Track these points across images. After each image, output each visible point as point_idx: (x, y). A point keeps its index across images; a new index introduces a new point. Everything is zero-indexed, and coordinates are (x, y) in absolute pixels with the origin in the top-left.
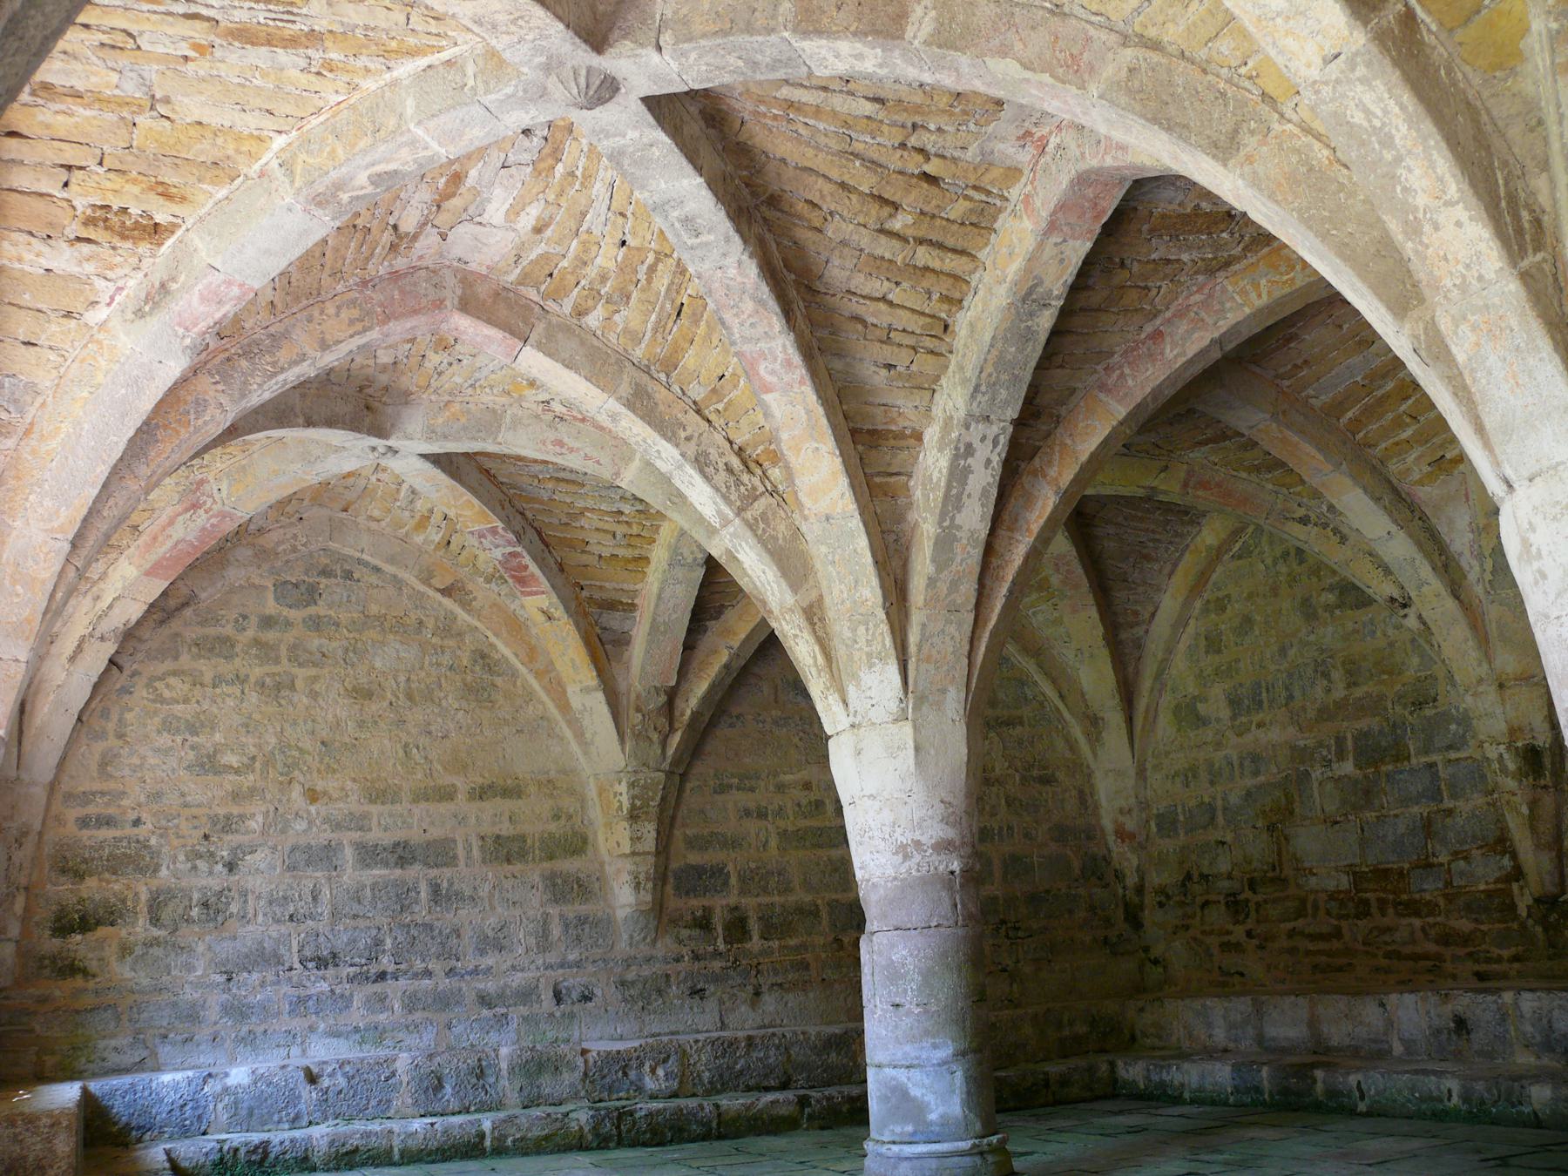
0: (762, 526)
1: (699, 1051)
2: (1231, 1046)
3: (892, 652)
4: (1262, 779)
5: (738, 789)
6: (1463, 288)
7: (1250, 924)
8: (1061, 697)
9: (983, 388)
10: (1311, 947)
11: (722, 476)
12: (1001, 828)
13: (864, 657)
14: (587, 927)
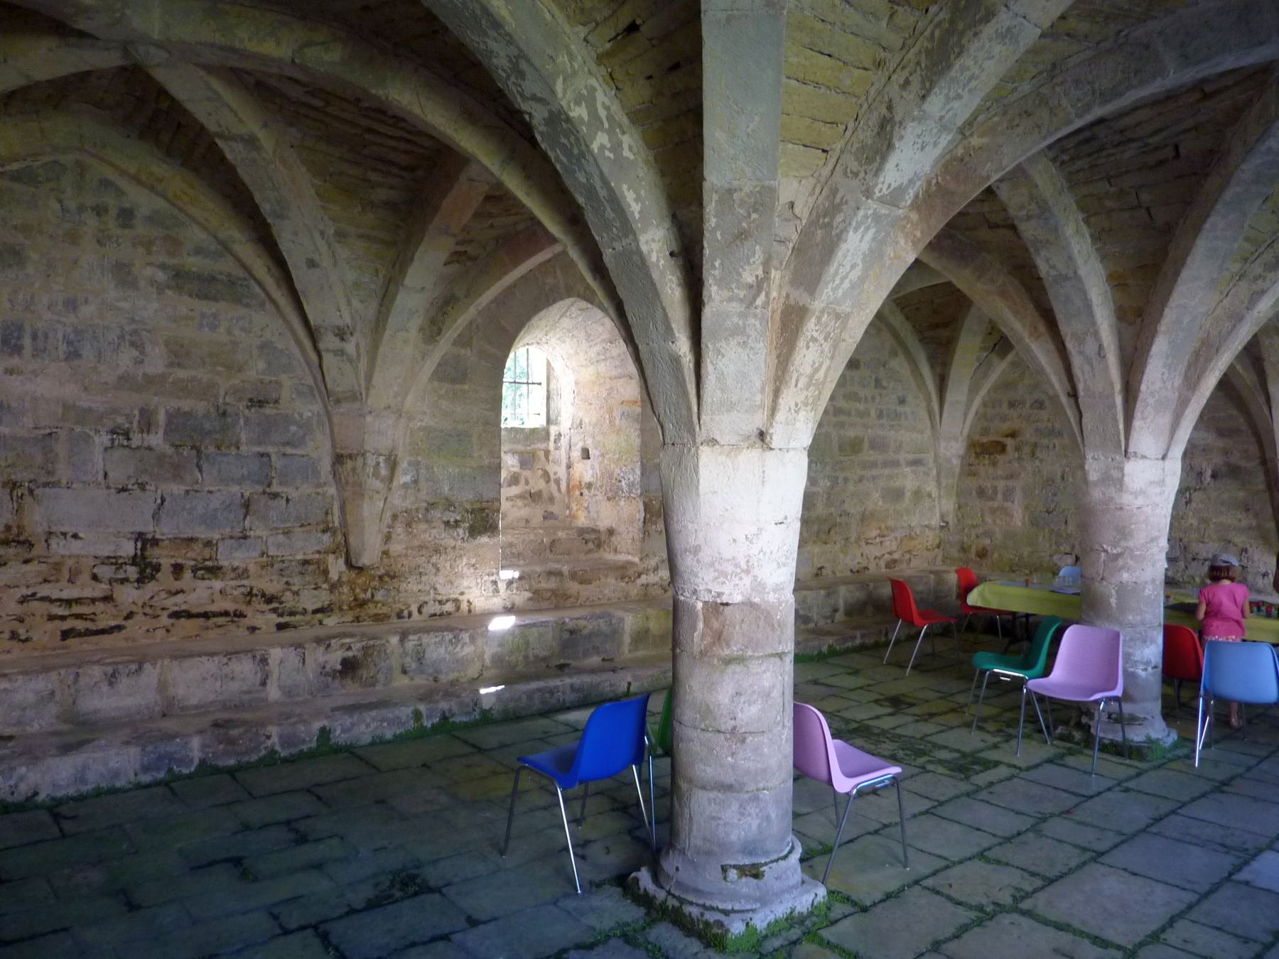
10: (60, 611)
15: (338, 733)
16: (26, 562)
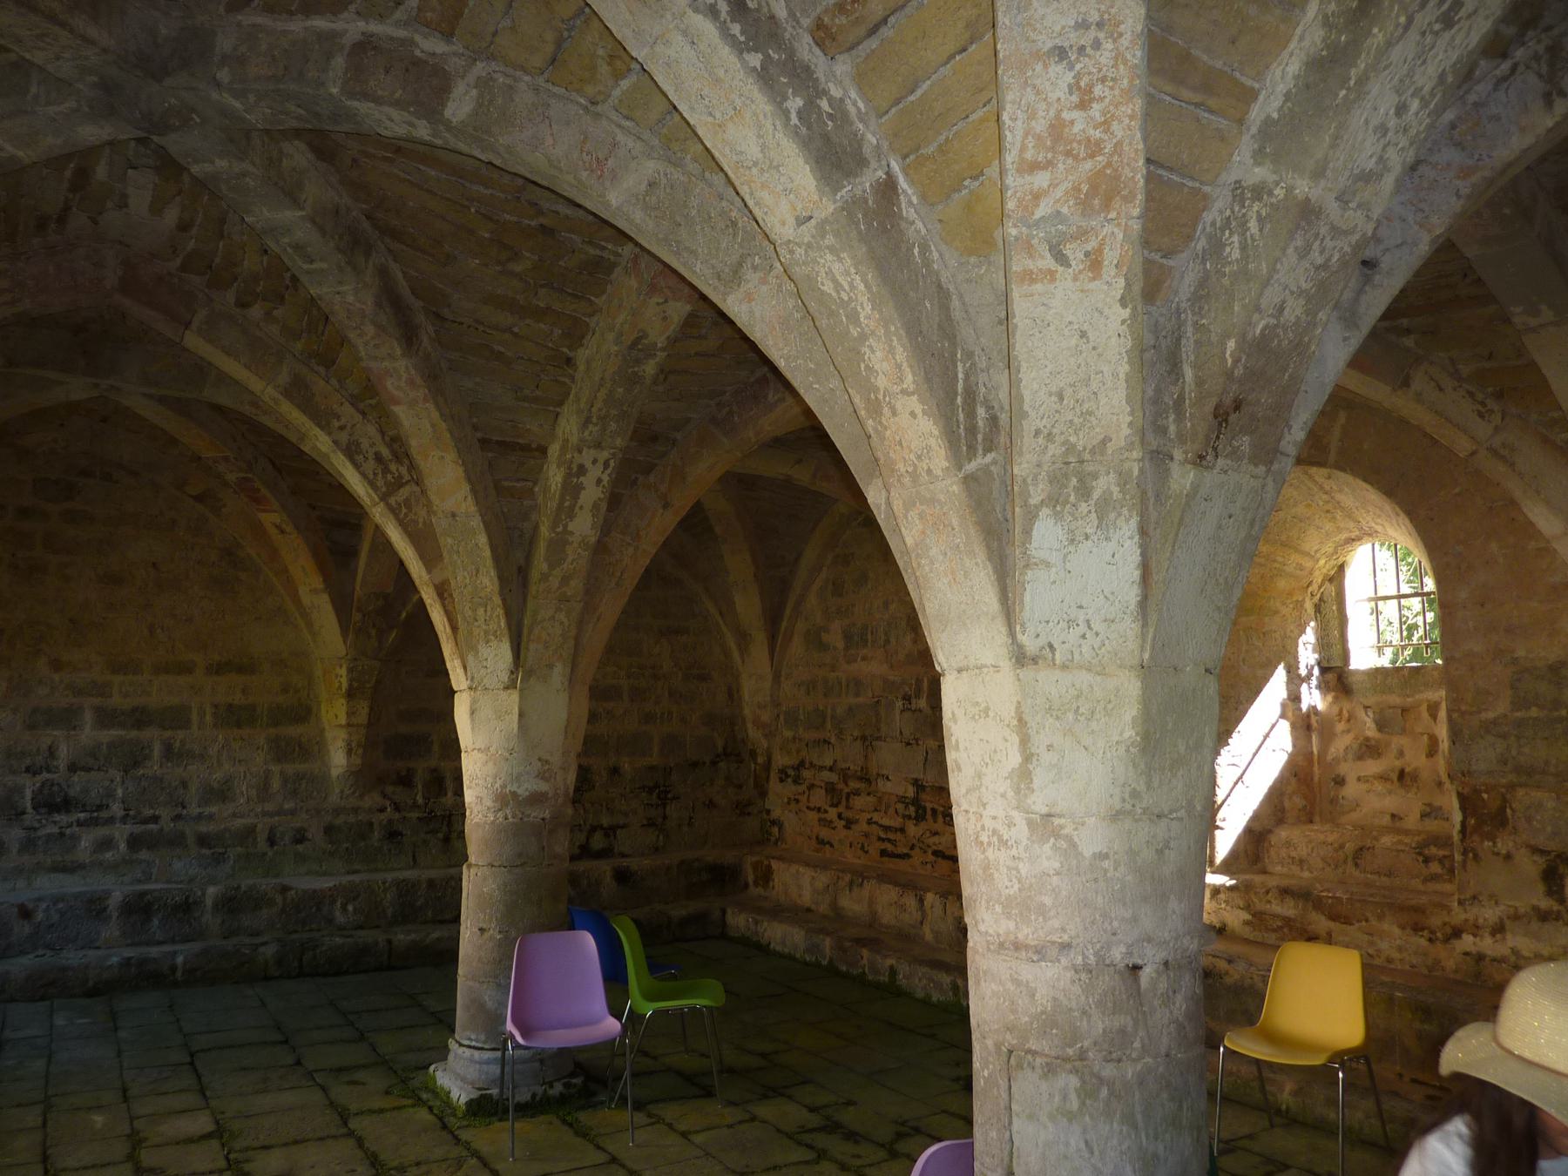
0: (404, 510)
2: (813, 907)
3: (506, 631)
4: (861, 700)
6: (914, 476)
7: (841, 809)
8: (721, 614)
9: (594, 420)
11: (370, 465)
12: (663, 714)
13: (482, 633)
15: (901, 976)
16: (869, 794)
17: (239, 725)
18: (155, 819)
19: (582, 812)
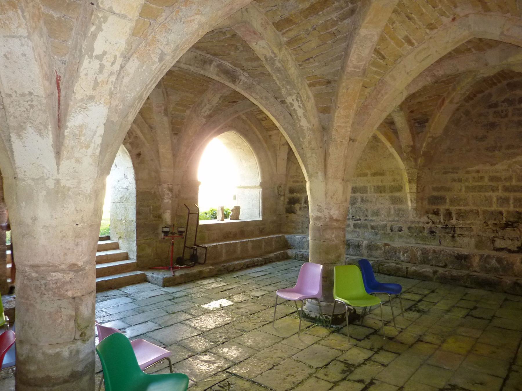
1: (417, 251)
5: (452, 173)
14: (401, 211)
17: (381, 192)
18: (360, 220)
19: (519, 232)
